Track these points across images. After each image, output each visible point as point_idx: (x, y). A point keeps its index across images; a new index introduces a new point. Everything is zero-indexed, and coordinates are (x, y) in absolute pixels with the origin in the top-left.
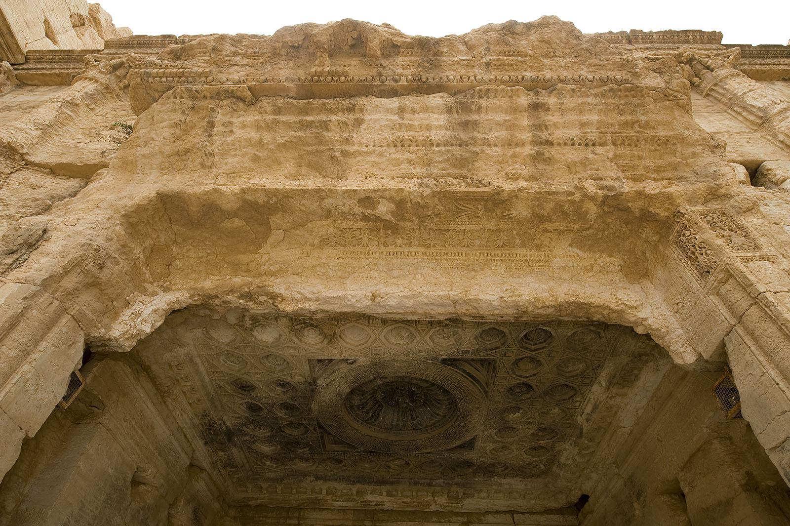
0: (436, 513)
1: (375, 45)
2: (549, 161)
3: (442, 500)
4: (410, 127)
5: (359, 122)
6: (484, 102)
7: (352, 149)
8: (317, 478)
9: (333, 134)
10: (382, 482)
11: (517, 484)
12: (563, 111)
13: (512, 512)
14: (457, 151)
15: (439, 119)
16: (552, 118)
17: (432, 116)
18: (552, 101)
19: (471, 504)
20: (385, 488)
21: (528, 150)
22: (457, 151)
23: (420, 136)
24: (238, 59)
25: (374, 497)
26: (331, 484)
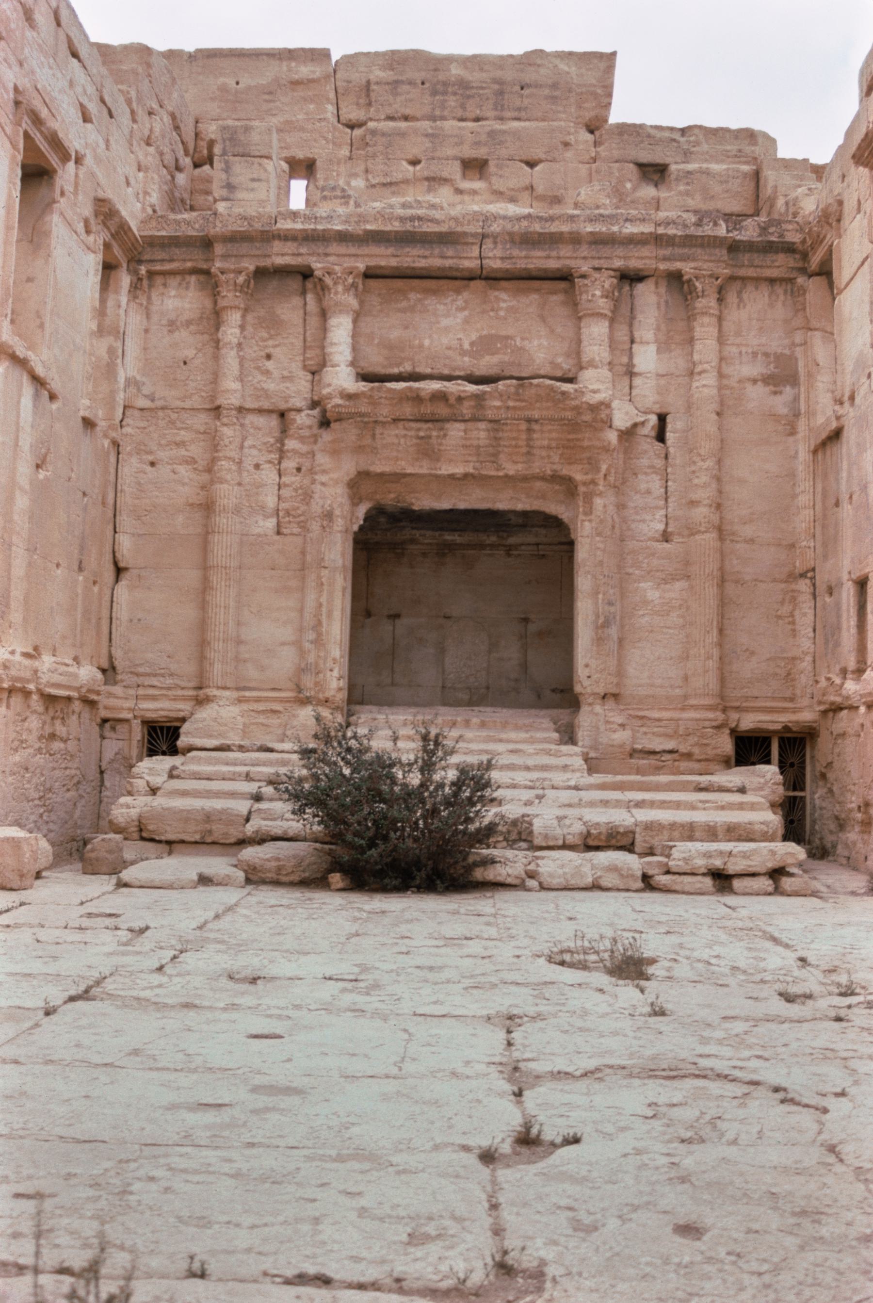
0: (489, 545)
1: (452, 400)
2: (534, 455)
3: (493, 539)
4: (470, 439)
5: (445, 435)
6: (505, 428)
7: (442, 448)
8: (413, 528)
9: (434, 441)
10: (455, 530)
11: (543, 531)
12: (542, 432)
13: (538, 544)
14: (491, 450)
15: (483, 435)
16: (535, 436)
17: (480, 433)
18: (536, 427)
19: (512, 540)
20: (456, 534)
21: (524, 450)
22: (491, 450)
23: (475, 442)
24: (383, 400)
25: (448, 537)
26: (422, 532)
